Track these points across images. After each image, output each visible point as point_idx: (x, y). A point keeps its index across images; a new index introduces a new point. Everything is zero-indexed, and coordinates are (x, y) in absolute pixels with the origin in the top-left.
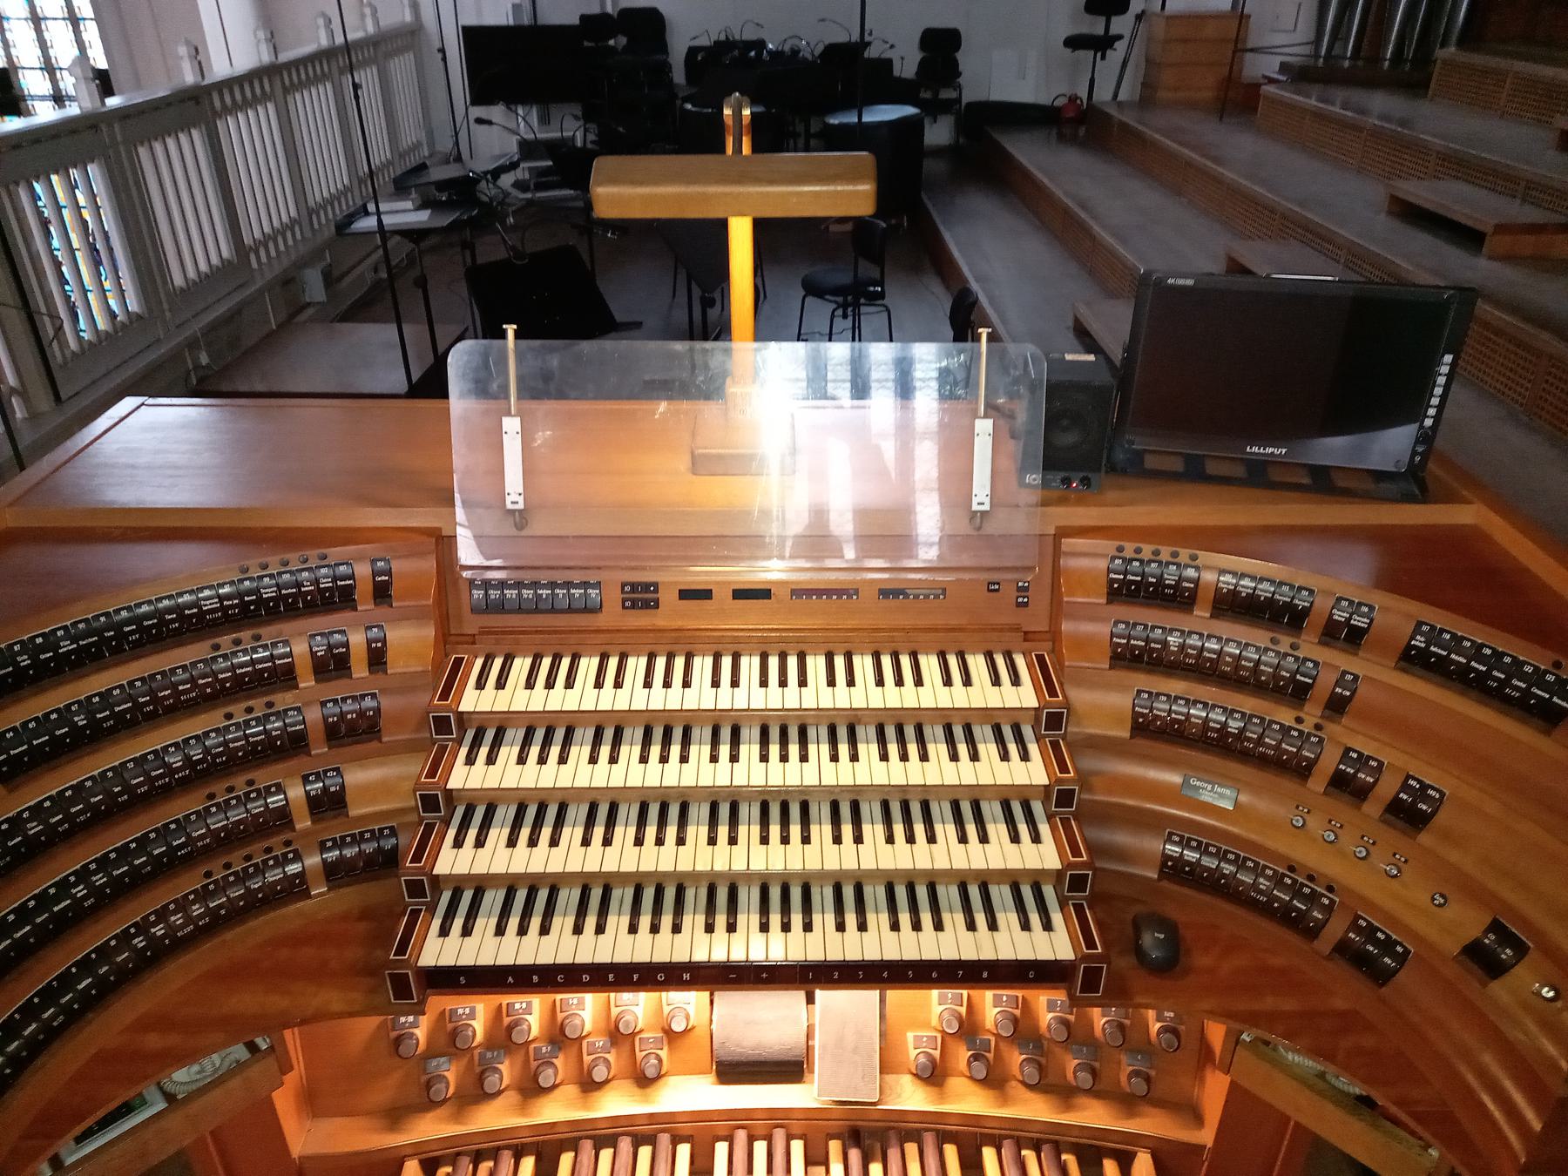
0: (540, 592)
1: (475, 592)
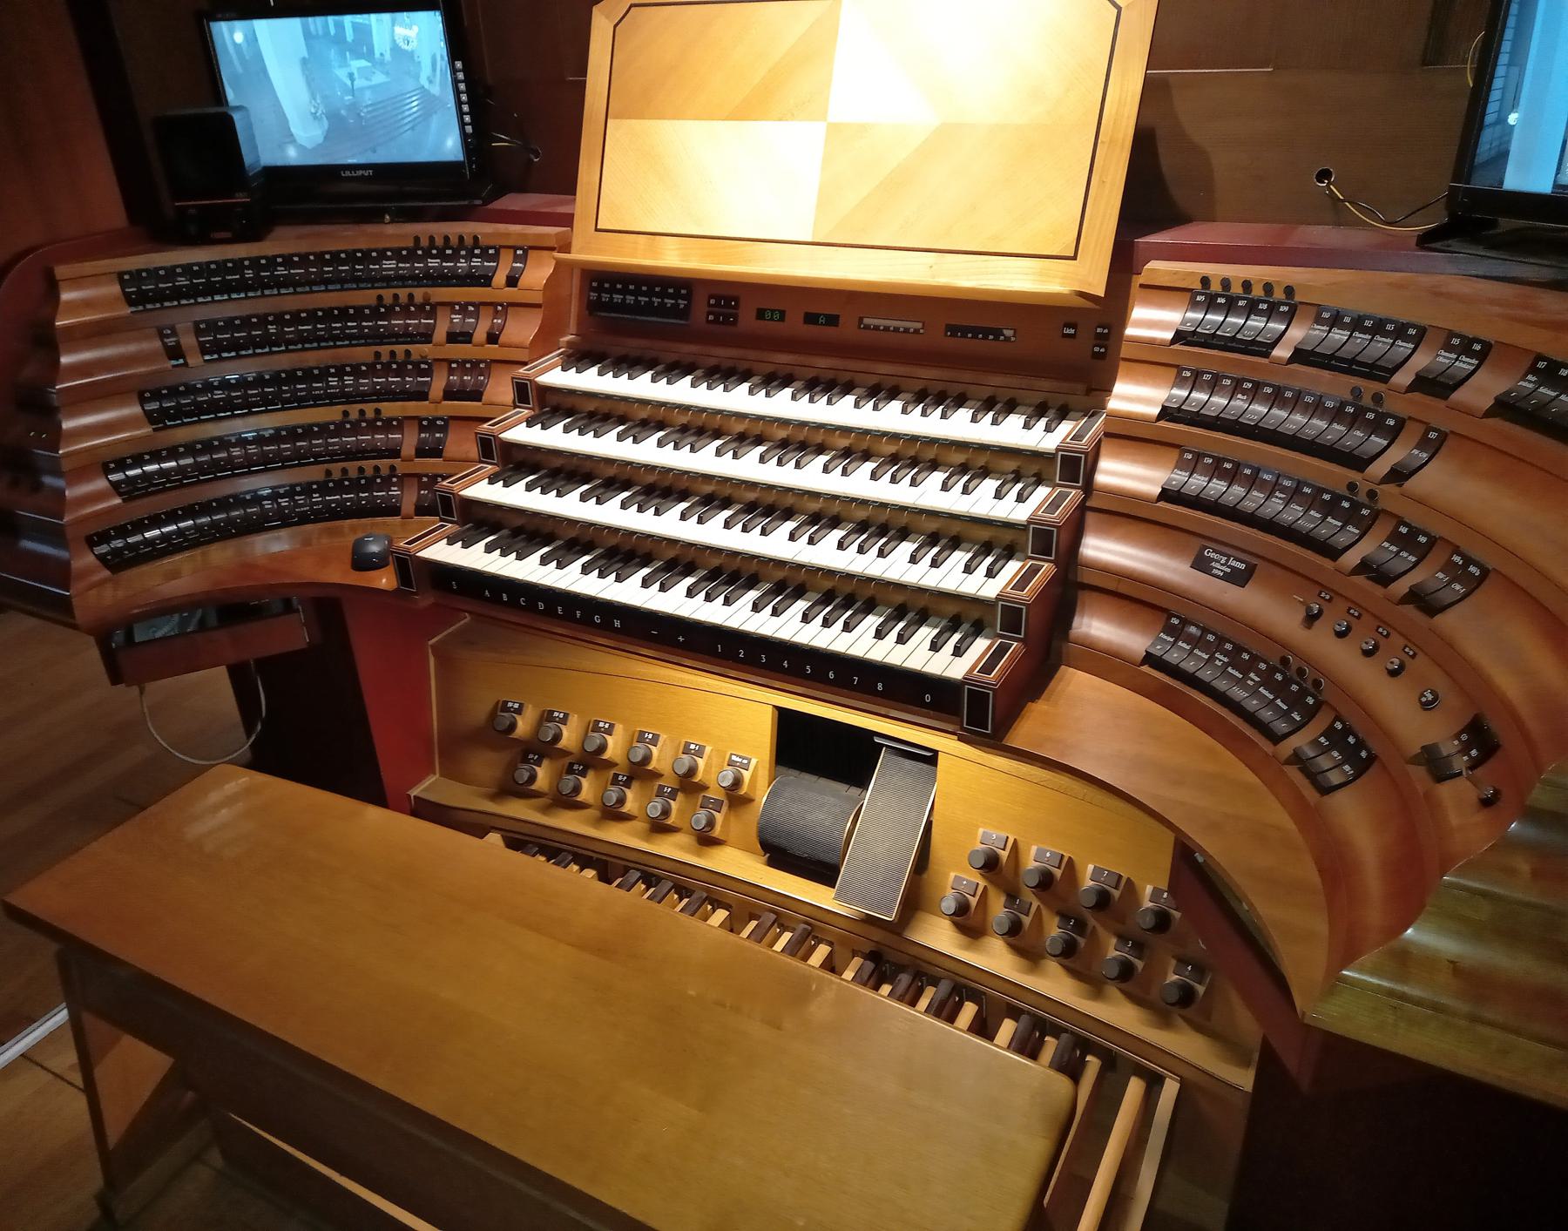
0: (639, 298)
1: (592, 294)
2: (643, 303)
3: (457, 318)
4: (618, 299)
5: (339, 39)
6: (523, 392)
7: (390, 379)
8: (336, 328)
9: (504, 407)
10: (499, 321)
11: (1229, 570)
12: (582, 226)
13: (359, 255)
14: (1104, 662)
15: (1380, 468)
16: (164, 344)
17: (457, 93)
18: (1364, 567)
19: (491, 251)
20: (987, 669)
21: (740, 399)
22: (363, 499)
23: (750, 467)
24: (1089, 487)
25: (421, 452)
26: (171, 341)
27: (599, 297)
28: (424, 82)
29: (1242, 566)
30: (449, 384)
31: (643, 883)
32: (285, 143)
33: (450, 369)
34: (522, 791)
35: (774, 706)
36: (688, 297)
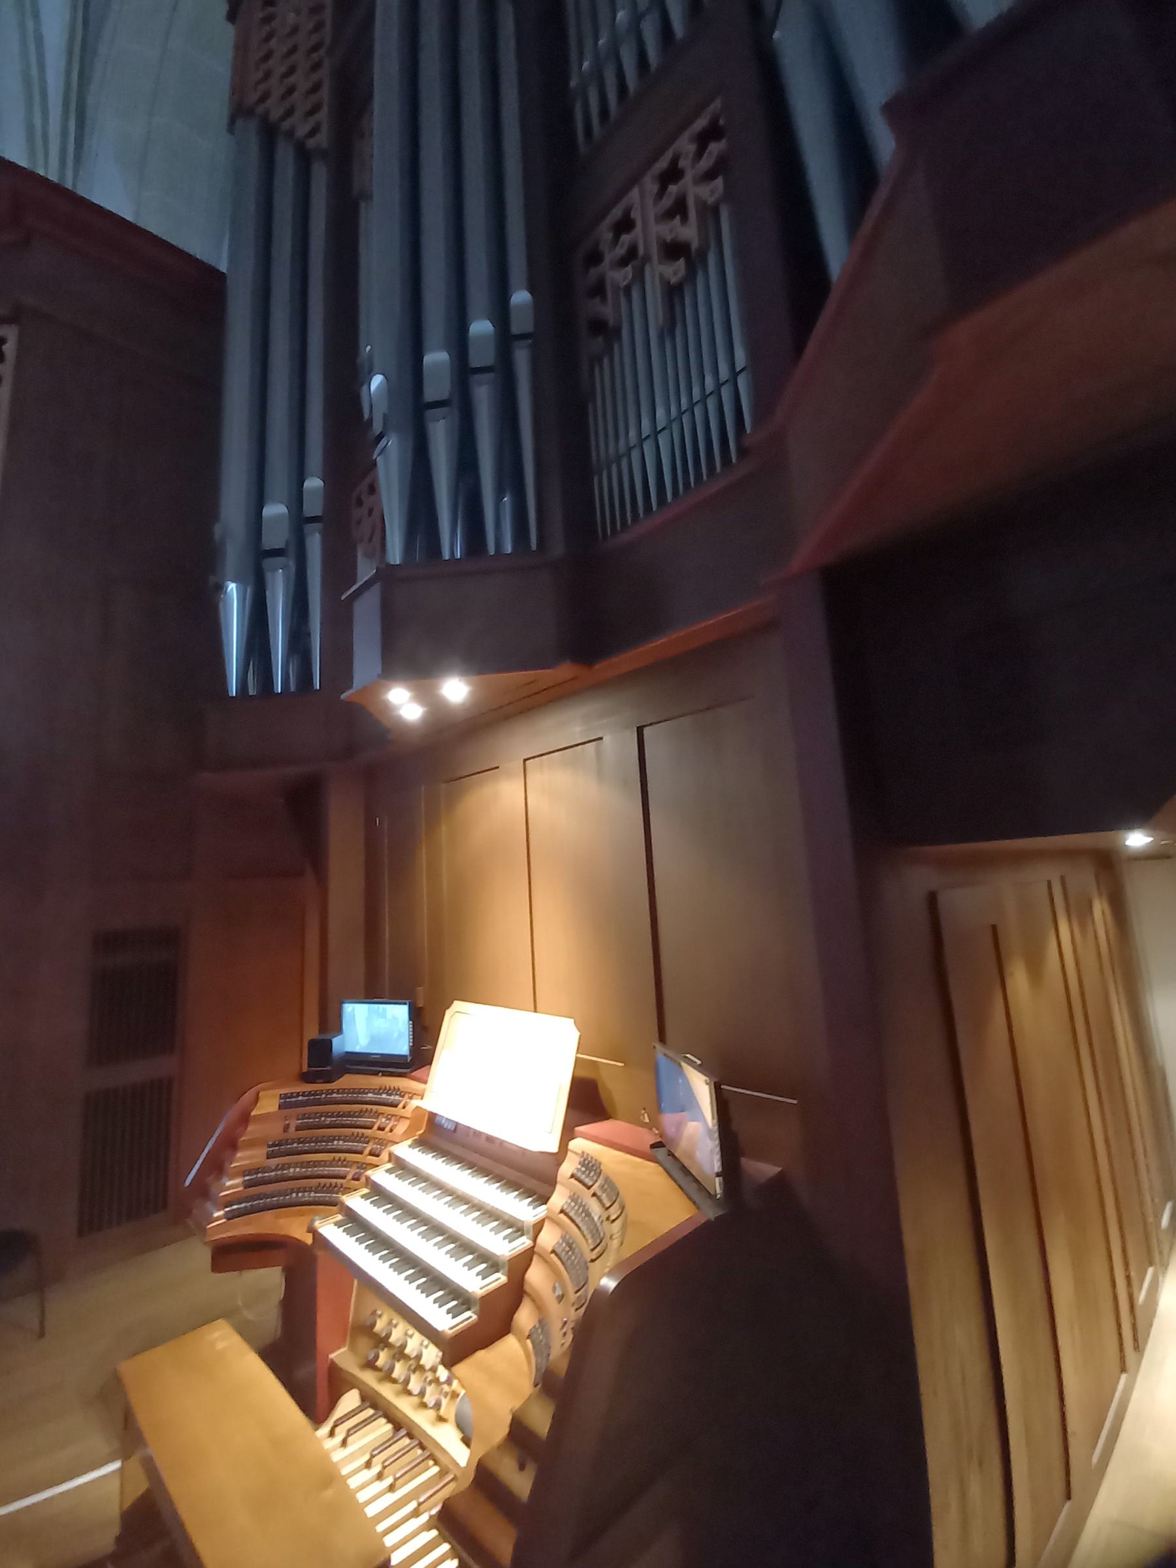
3: (384, 1120)
25: (354, 1179)
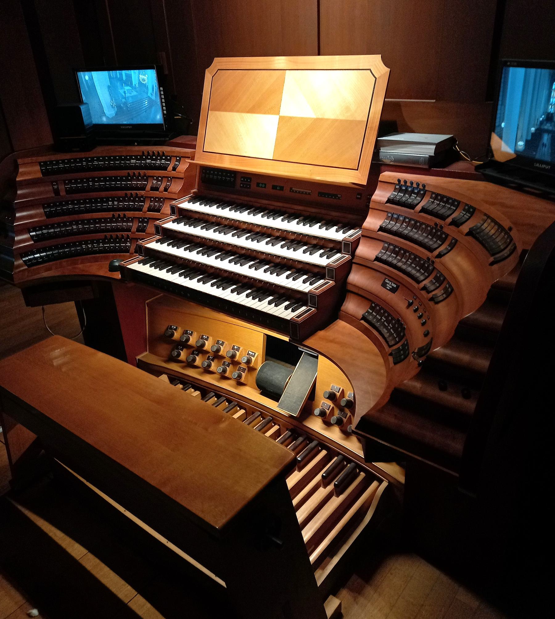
2: (224, 179)
3: (155, 182)
4: (215, 177)
5: (121, 79)
6: (174, 210)
7: (130, 203)
8: (113, 184)
9: (167, 215)
10: (169, 184)
11: (391, 287)
12: (198, 150)
13: (123, 157)
14: (351, 319)
15: (436, 252)
16: (53, 188)
17: (161, 99)
18: (424, 288)
19: (168, 158)
20: (298, 317)
21: (244, 217)
22: (117, 246)
23: (243, 242)
24: (353, 254)
25: (138, 230)
26: (55, 187)
27: (205, 176)
28: (149, 95)
29: (395, 286)
30: (150, 206)
31: (215, 397)
32: (103, 116)
33: (151, 200)
34: (174, 359)
35: (264, 333)
36: (235, 177)
